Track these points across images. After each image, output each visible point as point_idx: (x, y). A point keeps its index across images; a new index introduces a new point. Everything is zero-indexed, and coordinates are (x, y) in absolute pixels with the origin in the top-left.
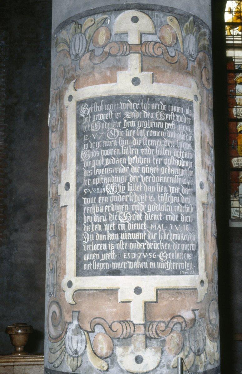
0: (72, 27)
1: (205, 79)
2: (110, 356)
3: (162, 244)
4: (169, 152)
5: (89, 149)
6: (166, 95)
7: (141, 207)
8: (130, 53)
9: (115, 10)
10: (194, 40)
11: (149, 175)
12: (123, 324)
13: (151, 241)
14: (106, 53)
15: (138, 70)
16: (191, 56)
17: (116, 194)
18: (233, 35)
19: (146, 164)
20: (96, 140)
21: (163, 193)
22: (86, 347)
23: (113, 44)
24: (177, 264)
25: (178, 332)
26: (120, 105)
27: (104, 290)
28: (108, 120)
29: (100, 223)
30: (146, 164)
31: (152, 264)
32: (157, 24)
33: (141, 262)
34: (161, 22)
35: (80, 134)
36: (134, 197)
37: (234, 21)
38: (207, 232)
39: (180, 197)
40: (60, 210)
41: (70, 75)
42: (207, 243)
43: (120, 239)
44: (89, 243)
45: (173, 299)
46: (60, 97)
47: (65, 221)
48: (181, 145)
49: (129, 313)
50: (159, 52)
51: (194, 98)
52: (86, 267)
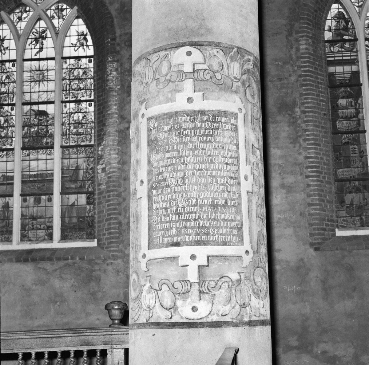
0: (143, 62)
1: (250, 95)
2: (173, 307)
3: (212, 222)
4: (217, 152)
5: (157, 153)
6: (214, 109)
7: (195, 194)
8: (185, 79)
9: (174, 47)
10: (238, 65)
11: (201, 170)
12: (183, 283)
13: (203, 220)
14: (168, 80)
15: (192, 91)
16: (235, 78)
17: (176, 186)
18: (334, 52)
19: (199, 162)
20: (161, 146)
21: (213, 183)
22: (156, 302)
23: (173, 73)
24: (224, 237)
25: (226, 289)
26: (178, 119)
27: (168, 258)
28: (170, 131)
29: (165, 208)
30: (199, 162)
31: (204, 237)
32: (206, 56)
33: (195, 236)
34: (210, 54)
35: (150, 142)
36: (189, 187)
37: (335, 39)
38: (251, 214)
39: (226, 186)
40: (137, 201)
41: (143, 99)
42: (252, 223)
43: (179, 219)
44: (157, 224)
45: (221, 263)
46: (136, 116)
47: (140, 209)
48: (227, 146)
49: (187, 275)
50: (208, 77)
51: (239, 110)
52: (155, 242)
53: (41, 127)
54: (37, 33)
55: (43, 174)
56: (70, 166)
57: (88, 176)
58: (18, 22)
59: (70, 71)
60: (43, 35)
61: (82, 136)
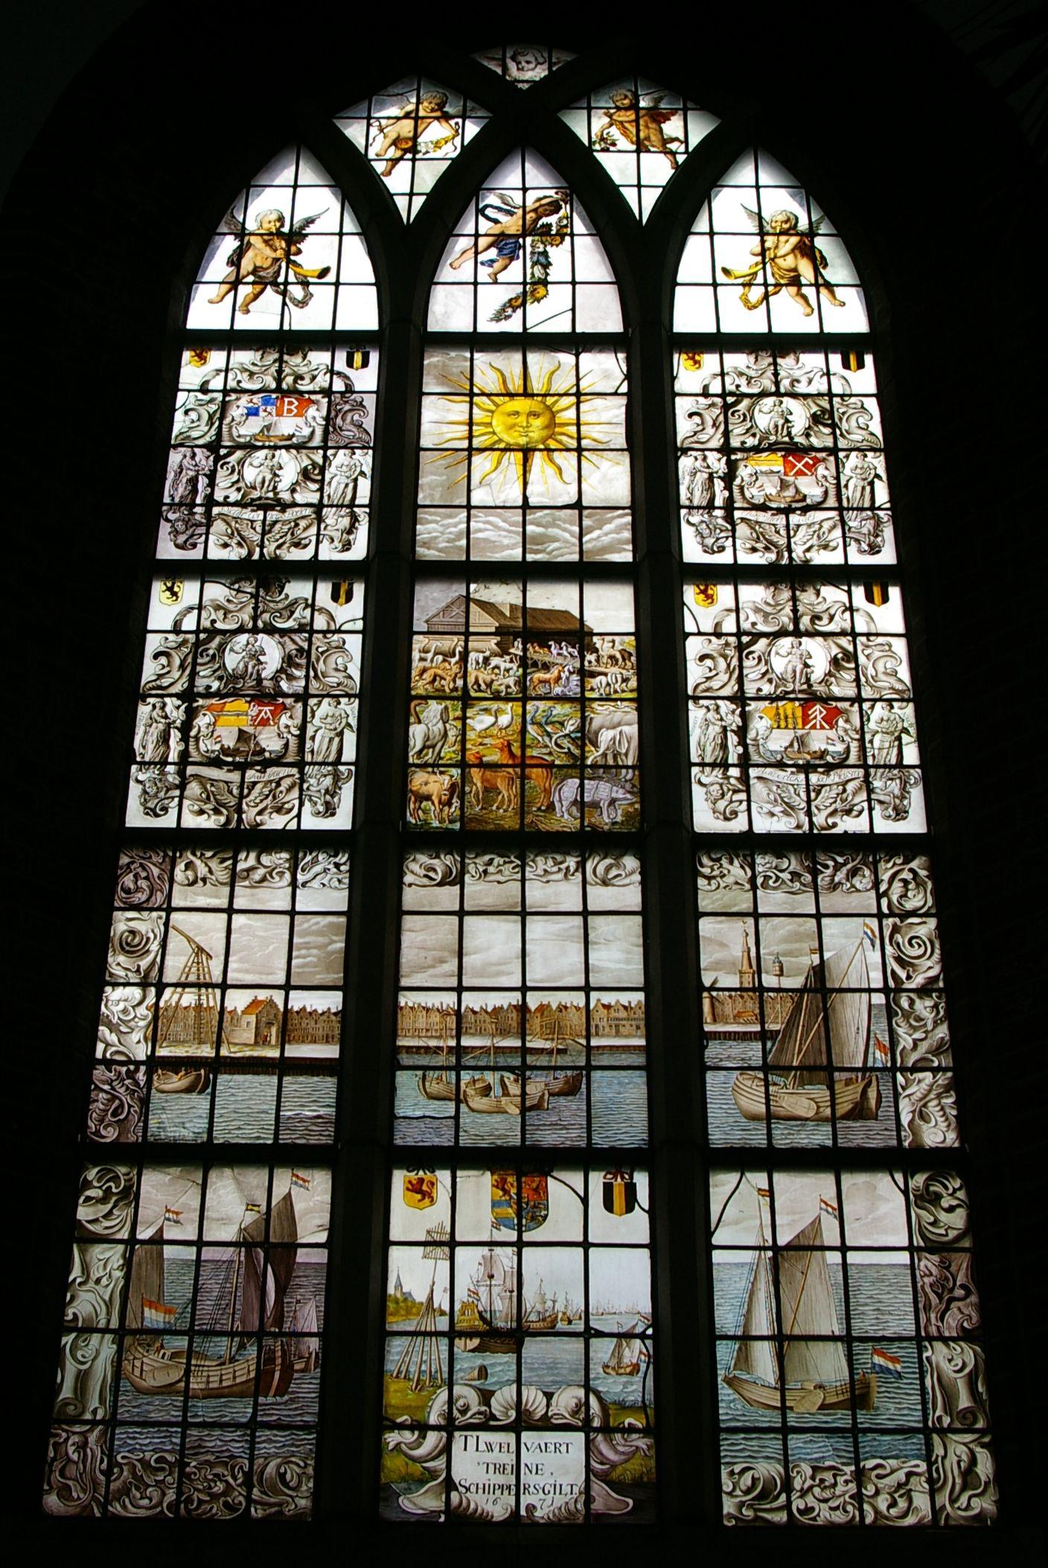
53: (542, 705)
54: (510, 213)
55: (563, 1008)
56: (767, 960)
57: (905, 1041)
58: (395, 162)
59: (726, 407)
60: (544, 220)
61: (834, 777)
